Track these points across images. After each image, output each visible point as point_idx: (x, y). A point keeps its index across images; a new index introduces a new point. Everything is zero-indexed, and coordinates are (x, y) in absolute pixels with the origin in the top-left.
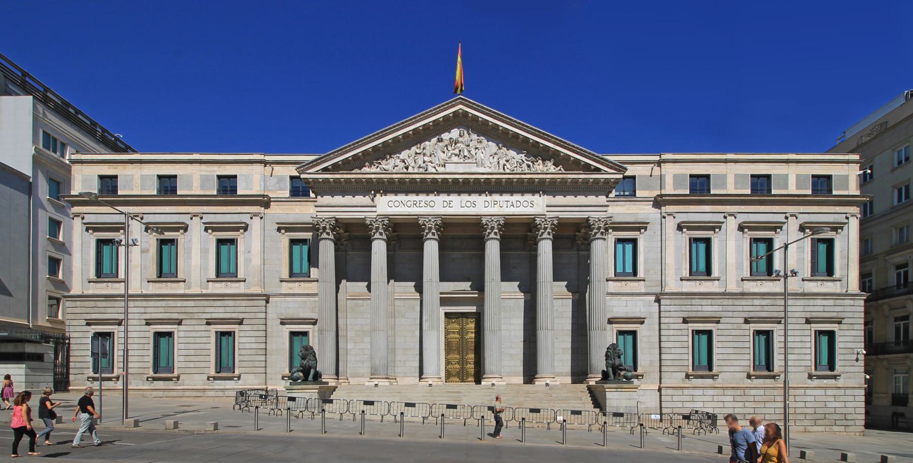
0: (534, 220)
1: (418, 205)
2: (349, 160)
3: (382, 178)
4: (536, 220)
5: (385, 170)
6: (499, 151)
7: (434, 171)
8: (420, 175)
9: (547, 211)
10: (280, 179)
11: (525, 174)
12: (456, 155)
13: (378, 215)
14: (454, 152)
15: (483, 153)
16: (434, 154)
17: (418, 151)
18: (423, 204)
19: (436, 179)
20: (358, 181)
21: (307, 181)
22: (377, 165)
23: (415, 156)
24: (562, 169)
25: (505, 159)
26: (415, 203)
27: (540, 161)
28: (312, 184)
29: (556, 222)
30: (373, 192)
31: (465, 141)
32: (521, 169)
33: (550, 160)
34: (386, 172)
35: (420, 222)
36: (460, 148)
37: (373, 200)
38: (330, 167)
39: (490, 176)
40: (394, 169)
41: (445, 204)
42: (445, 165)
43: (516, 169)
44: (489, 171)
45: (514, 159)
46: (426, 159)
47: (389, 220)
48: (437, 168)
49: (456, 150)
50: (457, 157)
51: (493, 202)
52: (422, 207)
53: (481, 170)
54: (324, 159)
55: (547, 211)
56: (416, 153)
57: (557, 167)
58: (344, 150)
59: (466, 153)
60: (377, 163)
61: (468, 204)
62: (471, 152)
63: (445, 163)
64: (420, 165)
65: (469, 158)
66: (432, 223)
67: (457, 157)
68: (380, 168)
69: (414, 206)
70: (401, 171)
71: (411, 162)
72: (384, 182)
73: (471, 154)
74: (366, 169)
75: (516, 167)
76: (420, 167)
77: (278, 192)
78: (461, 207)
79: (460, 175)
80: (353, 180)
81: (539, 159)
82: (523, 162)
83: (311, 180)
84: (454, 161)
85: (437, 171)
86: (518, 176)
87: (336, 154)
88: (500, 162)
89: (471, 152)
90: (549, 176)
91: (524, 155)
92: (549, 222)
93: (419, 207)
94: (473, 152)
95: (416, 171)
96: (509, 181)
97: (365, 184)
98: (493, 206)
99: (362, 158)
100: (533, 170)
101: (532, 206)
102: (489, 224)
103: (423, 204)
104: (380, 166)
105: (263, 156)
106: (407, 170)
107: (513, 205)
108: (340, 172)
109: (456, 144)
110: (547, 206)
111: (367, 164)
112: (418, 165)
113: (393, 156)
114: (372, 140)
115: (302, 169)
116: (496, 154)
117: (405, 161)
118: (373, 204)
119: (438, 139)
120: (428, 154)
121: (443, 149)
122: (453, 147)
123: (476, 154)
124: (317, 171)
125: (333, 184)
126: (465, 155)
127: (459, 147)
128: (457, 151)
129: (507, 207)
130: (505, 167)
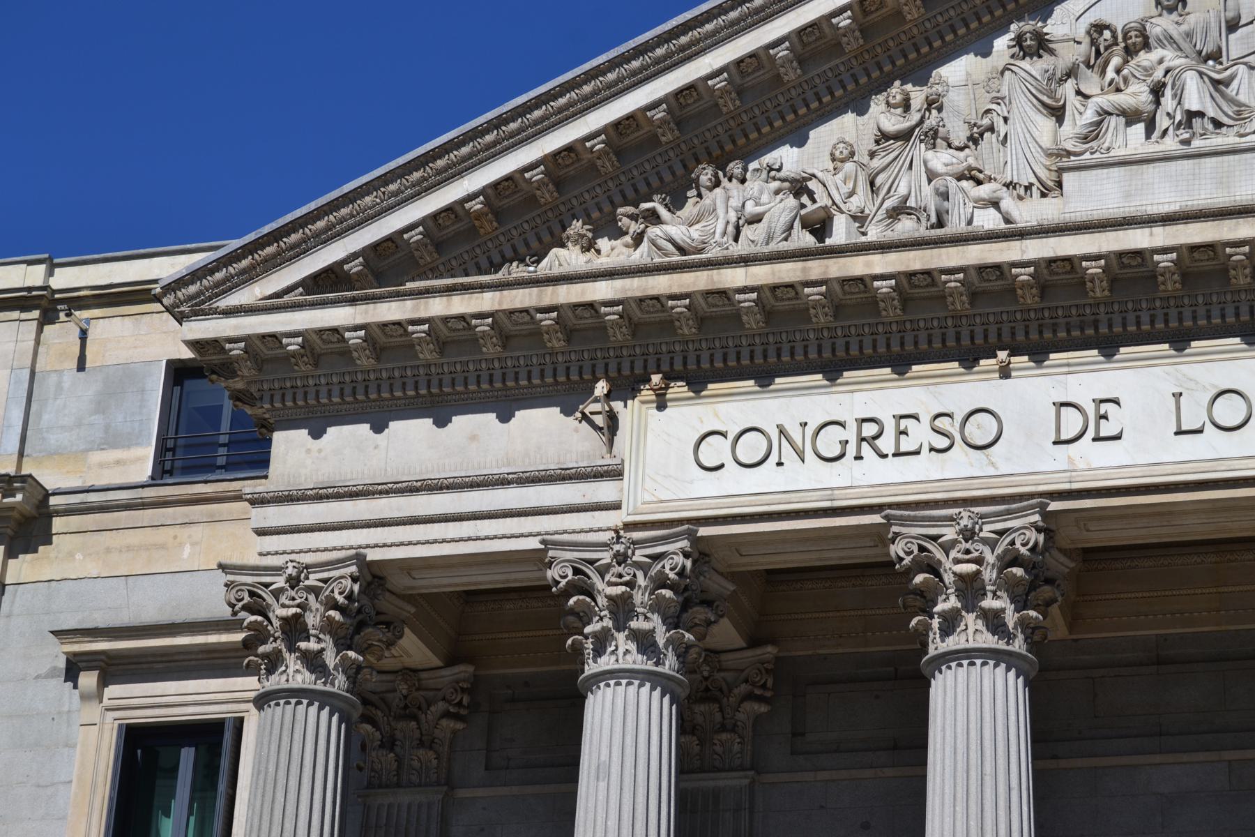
2: (468, 212)
3: (656, 298)
5: (682, 250)
7: (988, 220)
10: (127, 376)
12: (1131, 117)
13: (629, 526)
17: (893, 123)
19: (997, 267)
21: (215, 358)
22: (634, 227)
23: (872, 155)
28: (247, 370)
36: (1158, 74)
38: (355, 267)
40: (736, 240)
42: (1060, 185)
46: (941, 159)
47: (701, 552)
48: (1008, 203)
49: (1135, 87)
50: (1140, 128)
54: (320, 224)
56: (883, 137)
58: (440, 163)
59: (1195, 96)
60: (633, 217)
62: (1231, 90)
63: (1061, 171)
64: (906, 198)
65: (1218, 124)
66: (977, 548)
67: (1140, 128)
68: (653, 243)
70: (778, 246)
71: (846, 189)
72: (668, 324)
73: (1232, 101)
74: (567, 258)
76: (897, 213)
77: (96, 457)
78: (1179, 433)
80: (483, 326)
83: (236, 350)
84: (1118, 152)
85: (1008, 221)
87: (393, 187)
95: (874, 233)
97: (557, 343)
99: (546, 196)
104: (654, 231)
105: (42, 268)
106: (821, 240)
108: (410, 285)
109: (1130, 52)
111: (577, 226)
112: (889, 204)
113: (735, 167)
114: (610, 86)
115: (193, 289)
117: (812, 185)
119: (1019, 40)
121: (1051, 93)
124: (277, 295)
125: (365, 361)
126: (1195, 107)
127: (1148, 71)
128: (1137, 95)
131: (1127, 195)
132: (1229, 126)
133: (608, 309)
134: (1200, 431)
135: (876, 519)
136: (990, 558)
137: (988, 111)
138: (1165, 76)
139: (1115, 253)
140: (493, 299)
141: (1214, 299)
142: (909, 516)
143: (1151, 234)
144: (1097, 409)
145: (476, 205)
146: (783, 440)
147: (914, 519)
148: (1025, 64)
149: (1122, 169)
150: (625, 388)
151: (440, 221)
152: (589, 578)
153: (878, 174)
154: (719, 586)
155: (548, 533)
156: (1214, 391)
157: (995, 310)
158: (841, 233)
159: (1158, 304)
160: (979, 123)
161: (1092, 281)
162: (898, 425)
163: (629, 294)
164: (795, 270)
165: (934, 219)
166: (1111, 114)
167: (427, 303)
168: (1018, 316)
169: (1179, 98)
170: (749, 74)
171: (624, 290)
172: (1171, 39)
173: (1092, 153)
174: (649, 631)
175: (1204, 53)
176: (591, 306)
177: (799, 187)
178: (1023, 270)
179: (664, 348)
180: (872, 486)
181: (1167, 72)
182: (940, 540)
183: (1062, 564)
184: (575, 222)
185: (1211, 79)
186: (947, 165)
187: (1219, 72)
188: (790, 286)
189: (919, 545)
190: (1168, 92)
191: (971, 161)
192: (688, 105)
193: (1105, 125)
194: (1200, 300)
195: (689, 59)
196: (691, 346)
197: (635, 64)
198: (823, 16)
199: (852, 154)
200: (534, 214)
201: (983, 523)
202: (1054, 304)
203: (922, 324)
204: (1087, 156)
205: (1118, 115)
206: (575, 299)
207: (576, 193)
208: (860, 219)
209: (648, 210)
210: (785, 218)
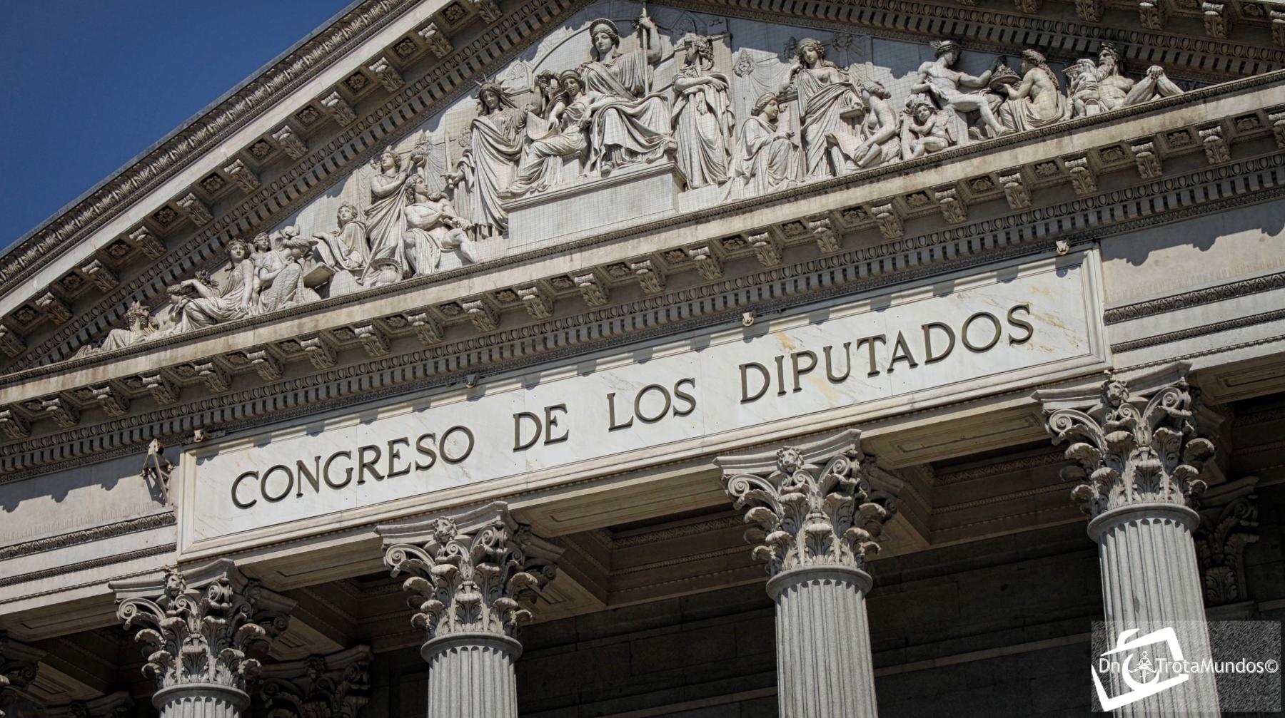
0: (1036, 414)
1: (382, 468)
4: (1047, 416)
5: (212, 319)
6: (805, 76)
7: (451, 263)
8: (368, 306)
9: (1117, 349)
11: (936, 163)
12: (566, 155)
14: (558, 141)
15: (711, 109)
16: (464, 178)
17: (383, 185)
18: (409, 455)
20: (75, 404)
22: (181, 300)
24: (1165, 81)
25: (837, 109)
26: (369, 456)
27: (1040, 75)
29: (1176, 399)
30: (153, 447)
31: (614, 76)
32: (919, 146)
33: (1095, 57)
34: (219, 325)
35: (388, 559)
37: (158, 493)
39: (737, 224)
41: (528, 427)
43: (890, 148)
44: (742, 192)
45: (882, 96)
46: (422, 211)
48: (468, 245)
50: (576, 163)
51: (788, 364)
52: (406, 472)
53: (703, 197)
55: (1117, 349)
56: (376, 197)
57: (1137, 77)
59: (615, 131)
61: (654, 403)
62: (643, 122)
65: (632, 153)
67: (576, 163)
69: (367, 474)
71: (344, 249)
73: (644, 132)
75: (896, 135)
76: (378, 265)
78: (613, 428)
79: (577, 256)
81: (1034, 63)
82: (938, 101)
85: (466, 260)
86: (894, 186)
88: (813, 132)
89: (643, 122)
90: (1079, 142)
91: (942, 60)
92: (1140, 407)
93: (391, 475)
94: (657, 116)
96: (857, 222)
98: (789, 385)
100: (998, 128)
101: (1020, 333)
102: (776, 495)
103: (409, 455)
107: (907, 357)
110: (1112, 318)
113: (261, 239)
116: (784, 97)
118: (158, 510)
120: (437, 186)
122: (553, 117)
123: (675, 123)
128: (572, 137)
129: (873, 373)
130: (835, 150)
131: (560, 226)
132: (643, 154)
133: (150, 379)
134: (629, 425)
135: (371, 535)
136: (466, 556)
137: (461, 164)
138: (592, 116)
139: (546, 280)
140: (57, 382)
141: (636, 307)
142: (396, 529)
143: (572, 260)
144: (548, 416)
145: (45, 301)
146: (302, 475)
147: (401, 530)
148: (484, 119)
149: (555, 204)
150: (176, 442)
151: (21, 318)
152: (152, 612)
153: (371, 230)
154: (277, 603)
155: (115, 579)
156: (641, 388)
157: (462, 340)
158: (342, 285)
159: (592, 317)
160: (454, 174)
161: (531, 306)
162: (391, 450)
163: (164, 364)
164: (292, 327)
165: (406, 267)
166: (549, 155)
167: (6, 392)
168: (482, 342)
169: (601, 132)
170: (265, 157)
171: (159, 361)
172: (603, 81)
173: (532, 193)
174: (200, 654)
175: (632, 89)
176: (137, 377)
177: (307, 251)
178: (472, 304)
179: (205, 405)
180: (372, 505)
181: (594, 112)
182: (426, 546)
183: (551, 551)
184: (133, 303)
185: (625, 114)
186: (421, 217)
187: (633, 107)
188: (292, 341)
189: (406, 552)
190: (596, 129)
191: (449, 211)
192: (216, 190)
193: (545, 165)
194: (625, 309)
195: (208, 150)
196: (225, 400)
197: (163, 161)
198: (313, 99)
199: (355, 215)
200: (100, 301)
201: (458, 528)
202: (509, 328)
203: (406, 359)
204: (528, 195)
205: (555, 156)
206: (121, 374)
207: (133, 277)
208: (357, 272)
209: (188, 286)
210: (290, 280)
